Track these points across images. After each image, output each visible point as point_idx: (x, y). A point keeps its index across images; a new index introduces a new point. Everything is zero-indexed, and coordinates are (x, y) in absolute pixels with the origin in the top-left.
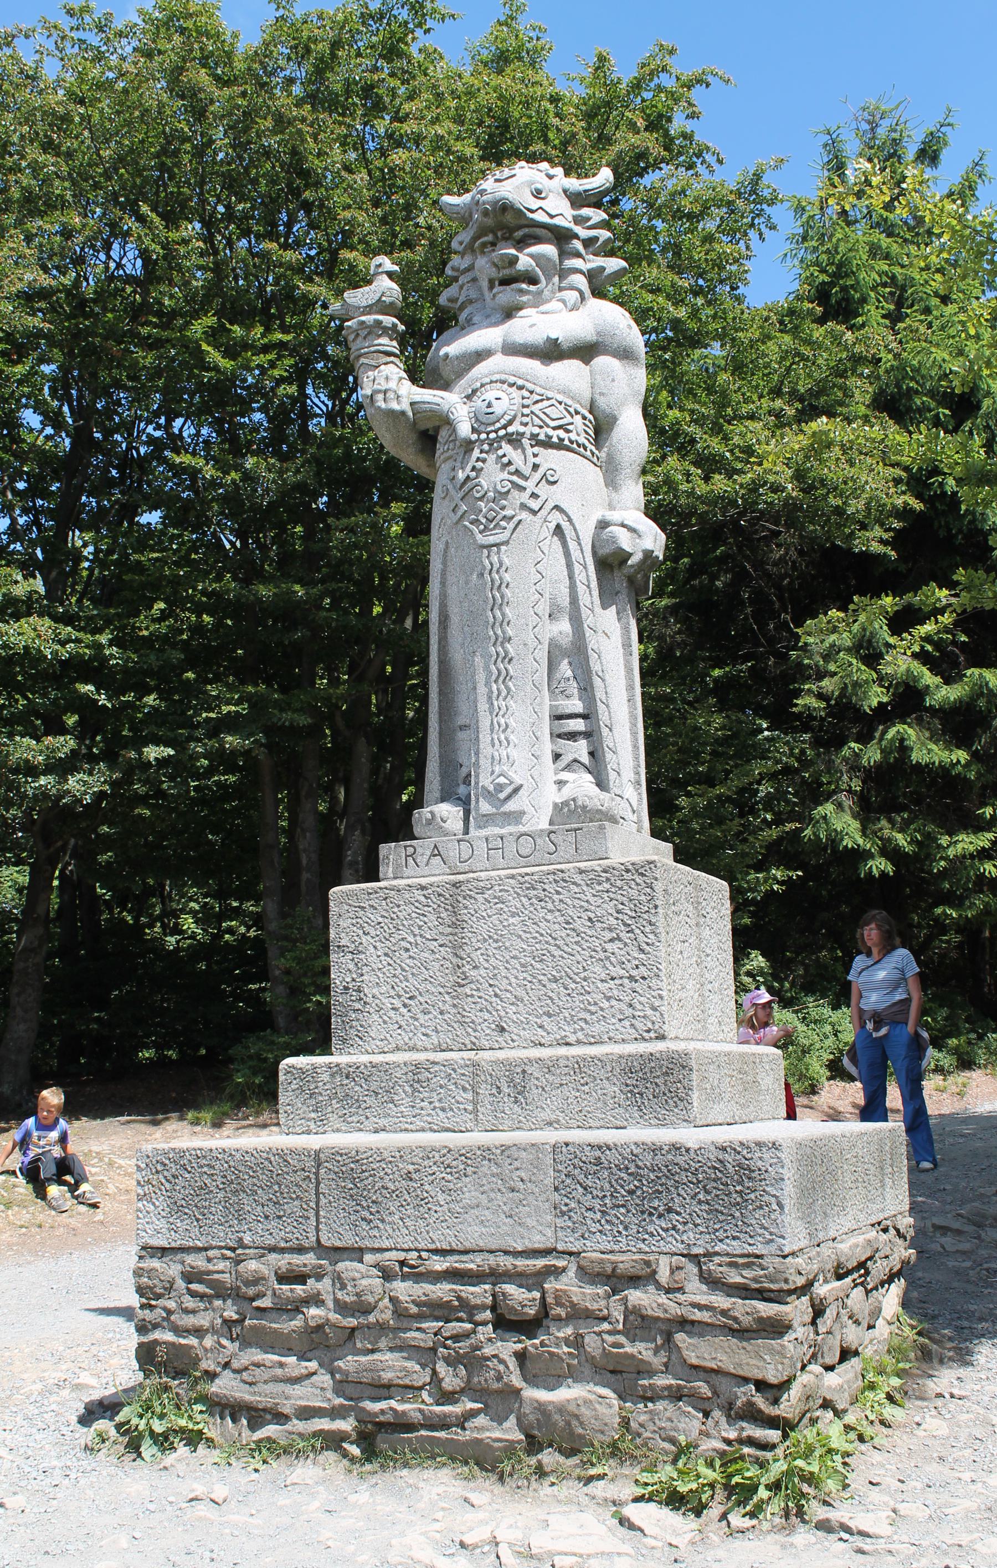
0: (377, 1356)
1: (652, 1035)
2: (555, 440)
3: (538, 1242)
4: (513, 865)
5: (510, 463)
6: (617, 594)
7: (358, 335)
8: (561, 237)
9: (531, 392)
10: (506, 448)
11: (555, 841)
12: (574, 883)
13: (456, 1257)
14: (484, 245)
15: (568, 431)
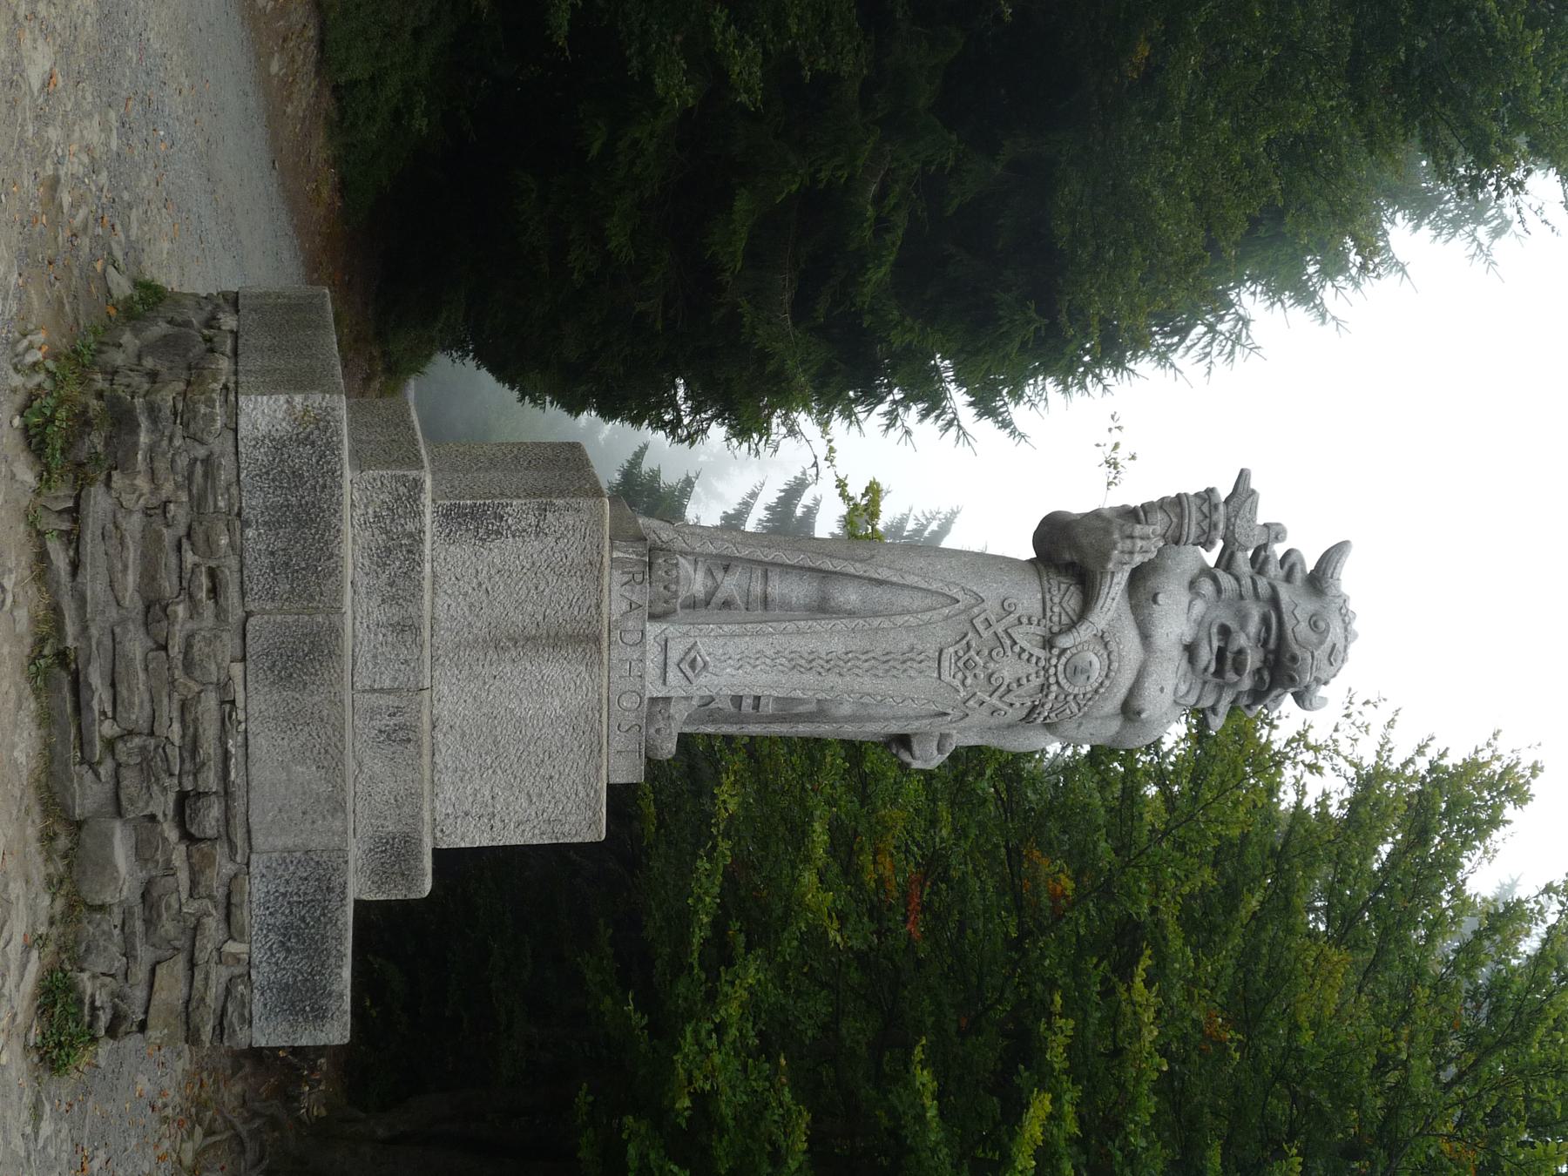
0: (142, 676)
1: (439, 835)
3: (259, 840)
5: (1020, 685)
10: (1036, 682)
13: (241, 759)
14: (1268, 630)
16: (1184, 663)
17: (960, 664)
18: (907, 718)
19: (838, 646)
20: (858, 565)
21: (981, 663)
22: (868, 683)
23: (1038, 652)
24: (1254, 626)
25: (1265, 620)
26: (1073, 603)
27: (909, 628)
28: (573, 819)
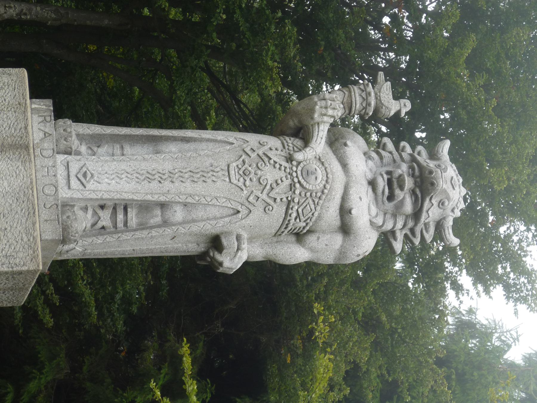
2: (290, 211)
4: (39, 182)
5: (278, 184)
6: (198, 245)
7: (363, 91)
8: (416, 215)
9: (320, 198)
10: (287, 182)
12: (27, 219)
14: (413, 169)
15: (296, 219)
16: (370, 190)
17: (241, 172)
18: (215, 218)
19: (168, 166)
21: (253, 171)
22: (188, 187)
23: (284, 164)
24: (404, 167)
25: (412, 168)
26: (298, 143)
27: (208, 156)
28: (21, 255)
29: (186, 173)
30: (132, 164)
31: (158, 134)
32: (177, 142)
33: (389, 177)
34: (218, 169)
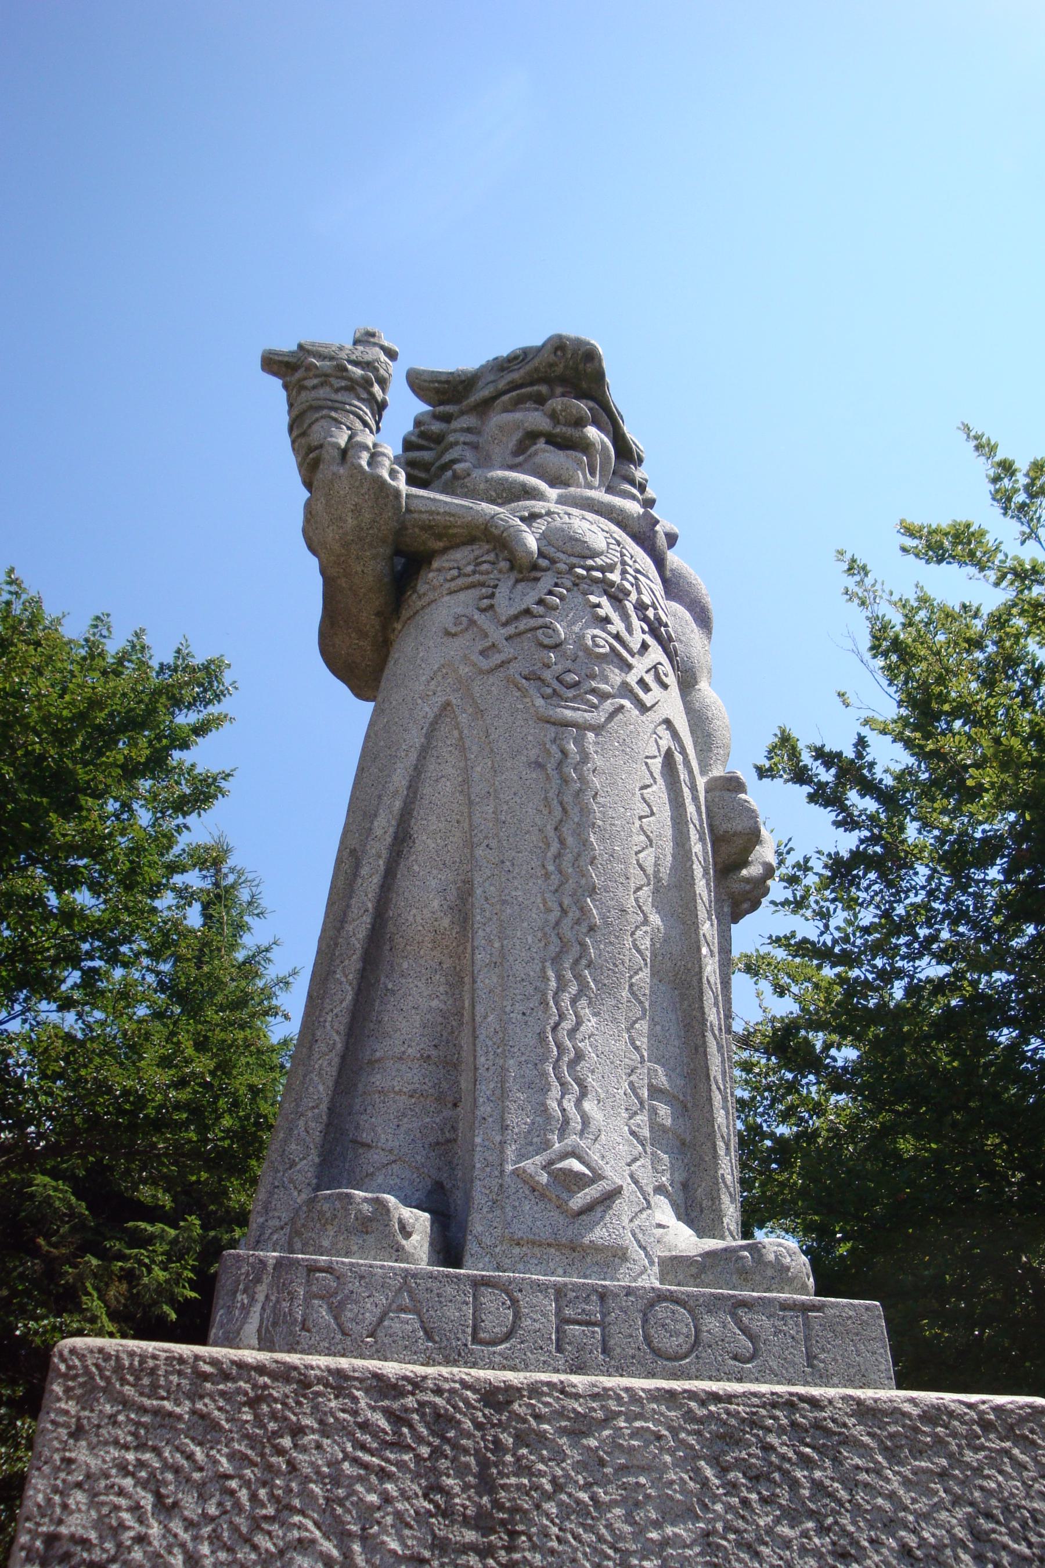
11: (754, 1327)
20: (364, 871)
29: (562, 842)
30: (519, 1007)
31: (367, 919)
32: (402, 870)
33: (542, 440)
34: (554, 749)
